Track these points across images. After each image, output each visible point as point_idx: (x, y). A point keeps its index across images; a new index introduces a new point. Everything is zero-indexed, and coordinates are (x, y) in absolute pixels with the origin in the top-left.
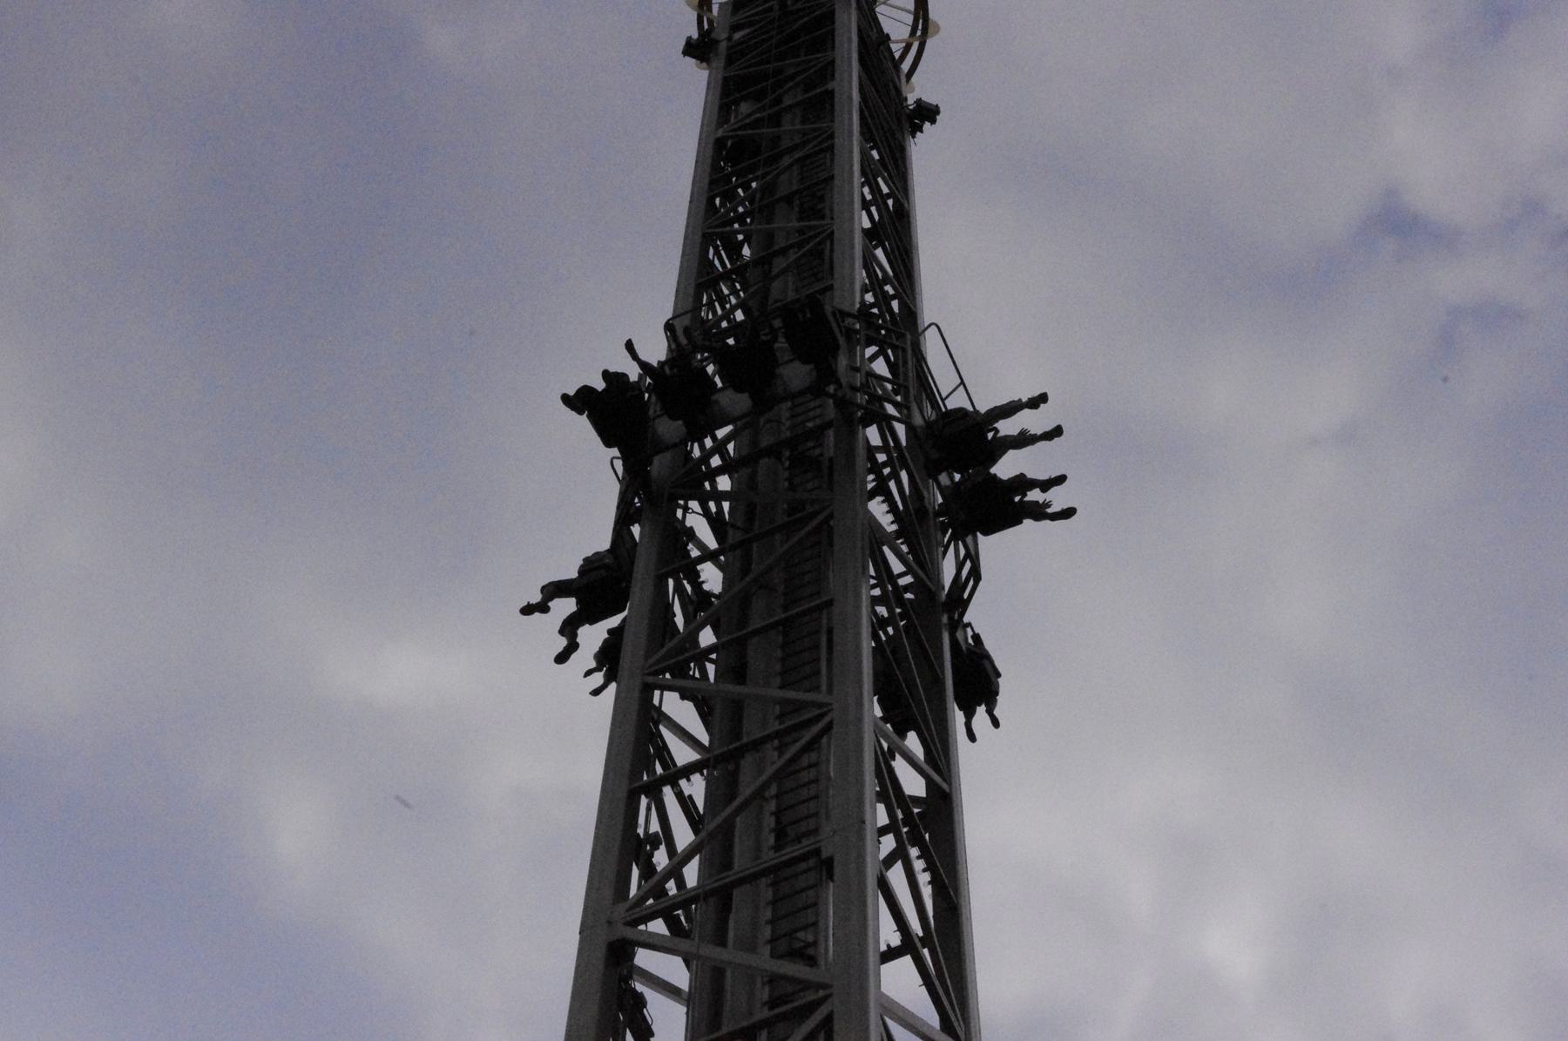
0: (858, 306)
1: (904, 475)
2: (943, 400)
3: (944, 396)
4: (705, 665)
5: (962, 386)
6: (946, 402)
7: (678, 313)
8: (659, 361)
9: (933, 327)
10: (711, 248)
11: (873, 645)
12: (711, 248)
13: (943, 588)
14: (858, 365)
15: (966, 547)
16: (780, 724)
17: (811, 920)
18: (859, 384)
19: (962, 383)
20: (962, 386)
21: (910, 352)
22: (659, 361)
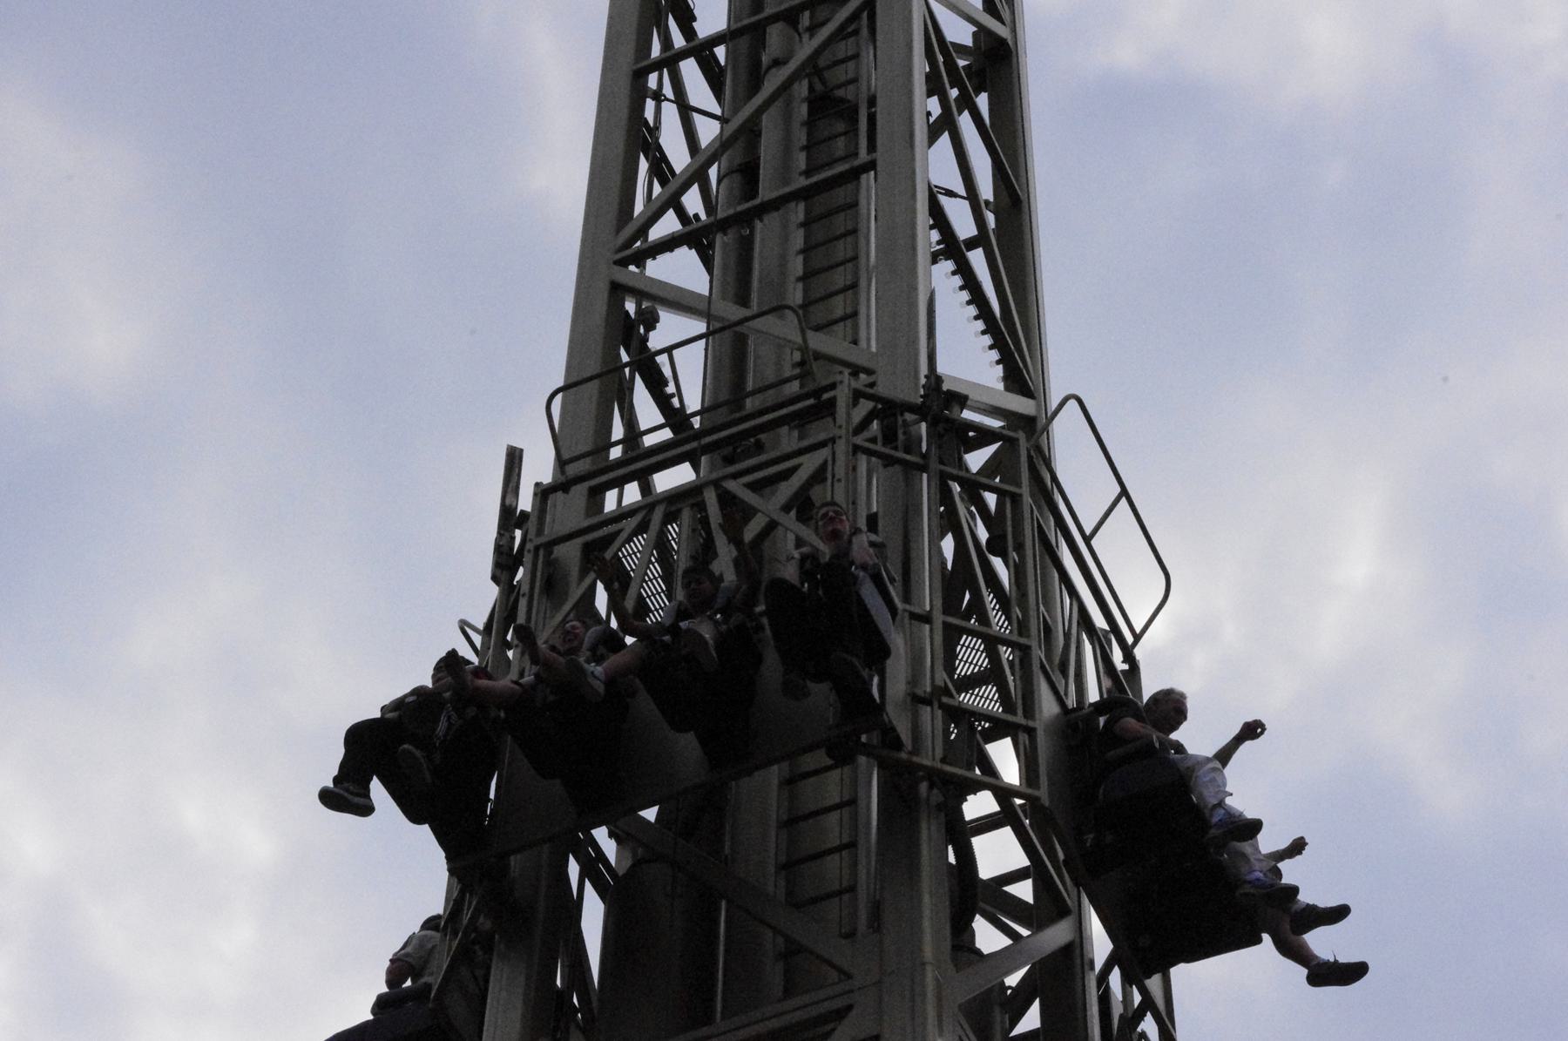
0: (923, 381)
1: (982, 101)
2: (1087, 540)
3: (1088, 532)
4: (656, 805)
5: (1124, 500)
6: (1094, 542)
7: (574, 379)
8: (537, 485)
9: (1072, 403)
10: (572, 860)
11: (928, 70)
12: (572, 860)
13: (1092, 967)
14: (928, 608)
15: (1144, 992)
16: (801, 438)
17: (851, 75)
18: (929, 689)
19: (1124, 493)
20: (1124, 500)
21: (1027, 500)
22: (537, 485)
